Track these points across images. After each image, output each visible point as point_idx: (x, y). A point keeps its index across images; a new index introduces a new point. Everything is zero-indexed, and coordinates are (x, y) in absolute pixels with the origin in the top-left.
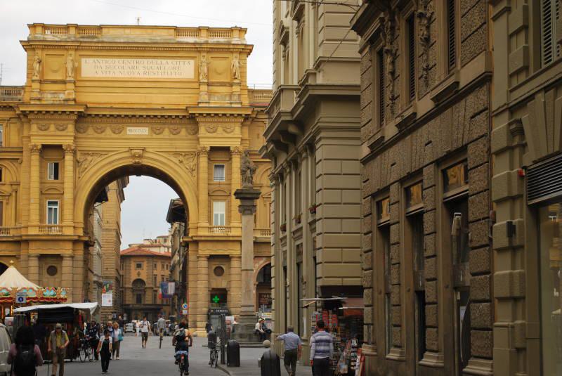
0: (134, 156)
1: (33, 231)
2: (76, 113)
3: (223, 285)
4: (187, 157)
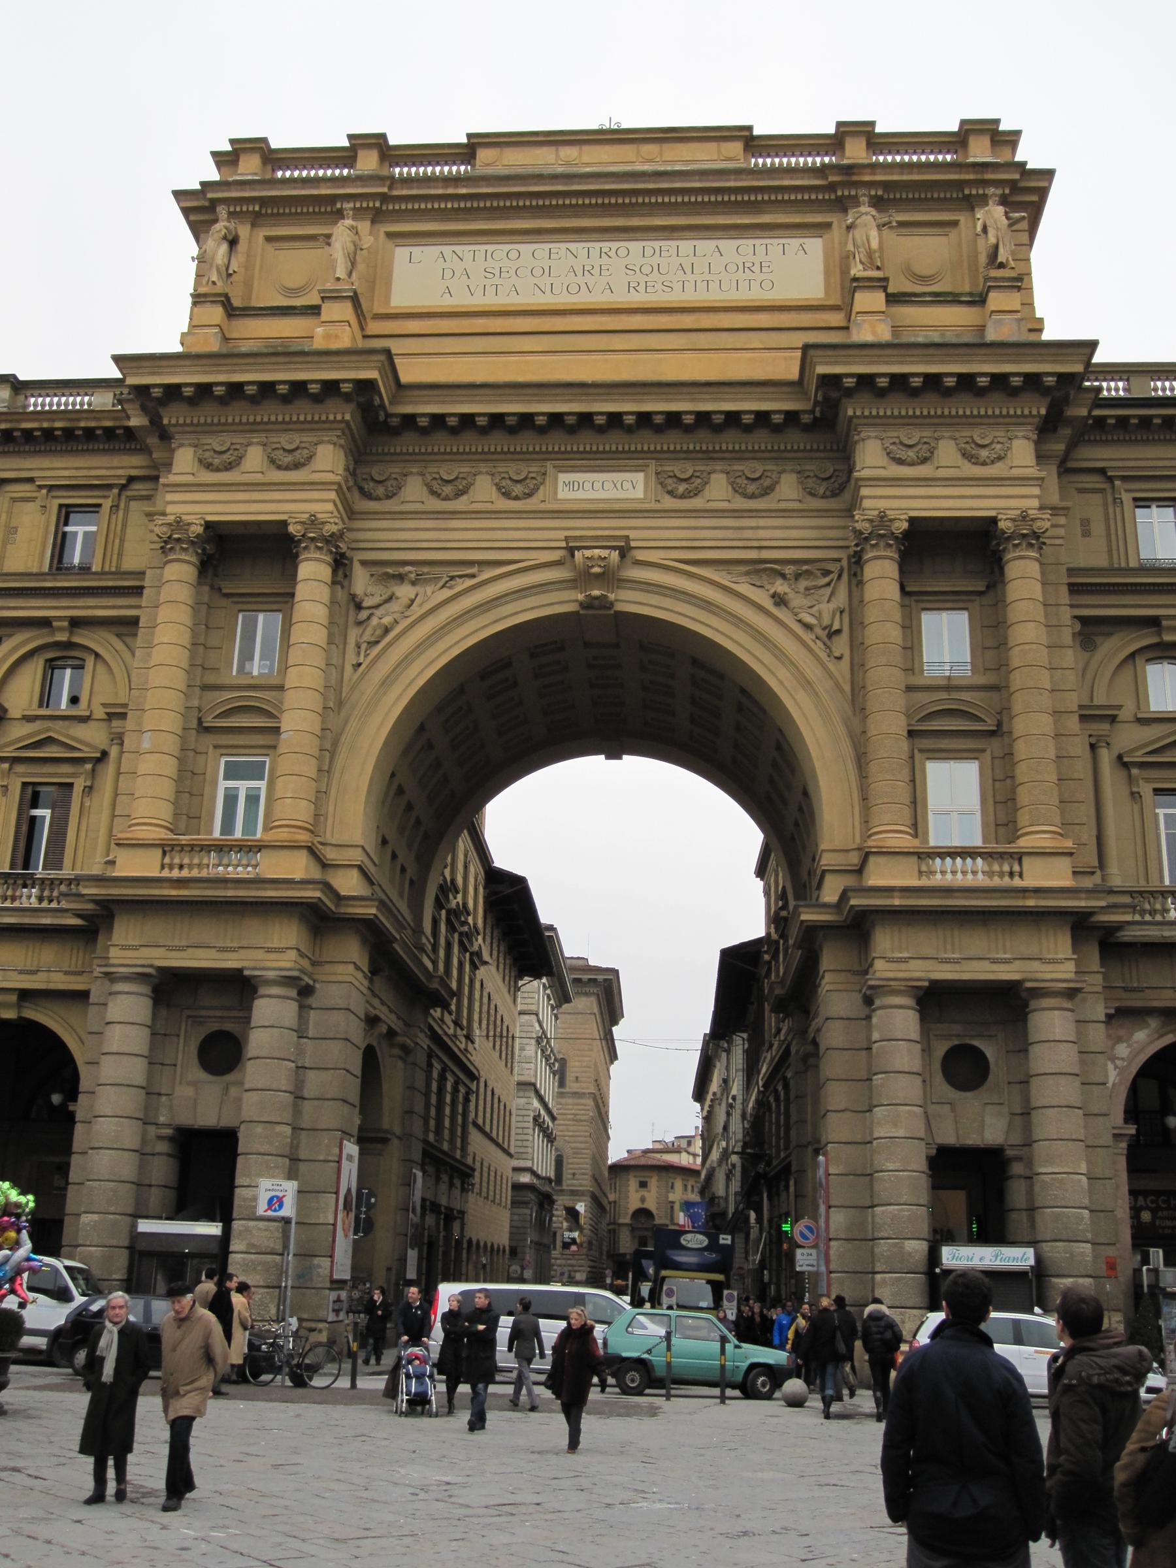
0: (584, 577)
2: (346, 388)
4: (803, 584)
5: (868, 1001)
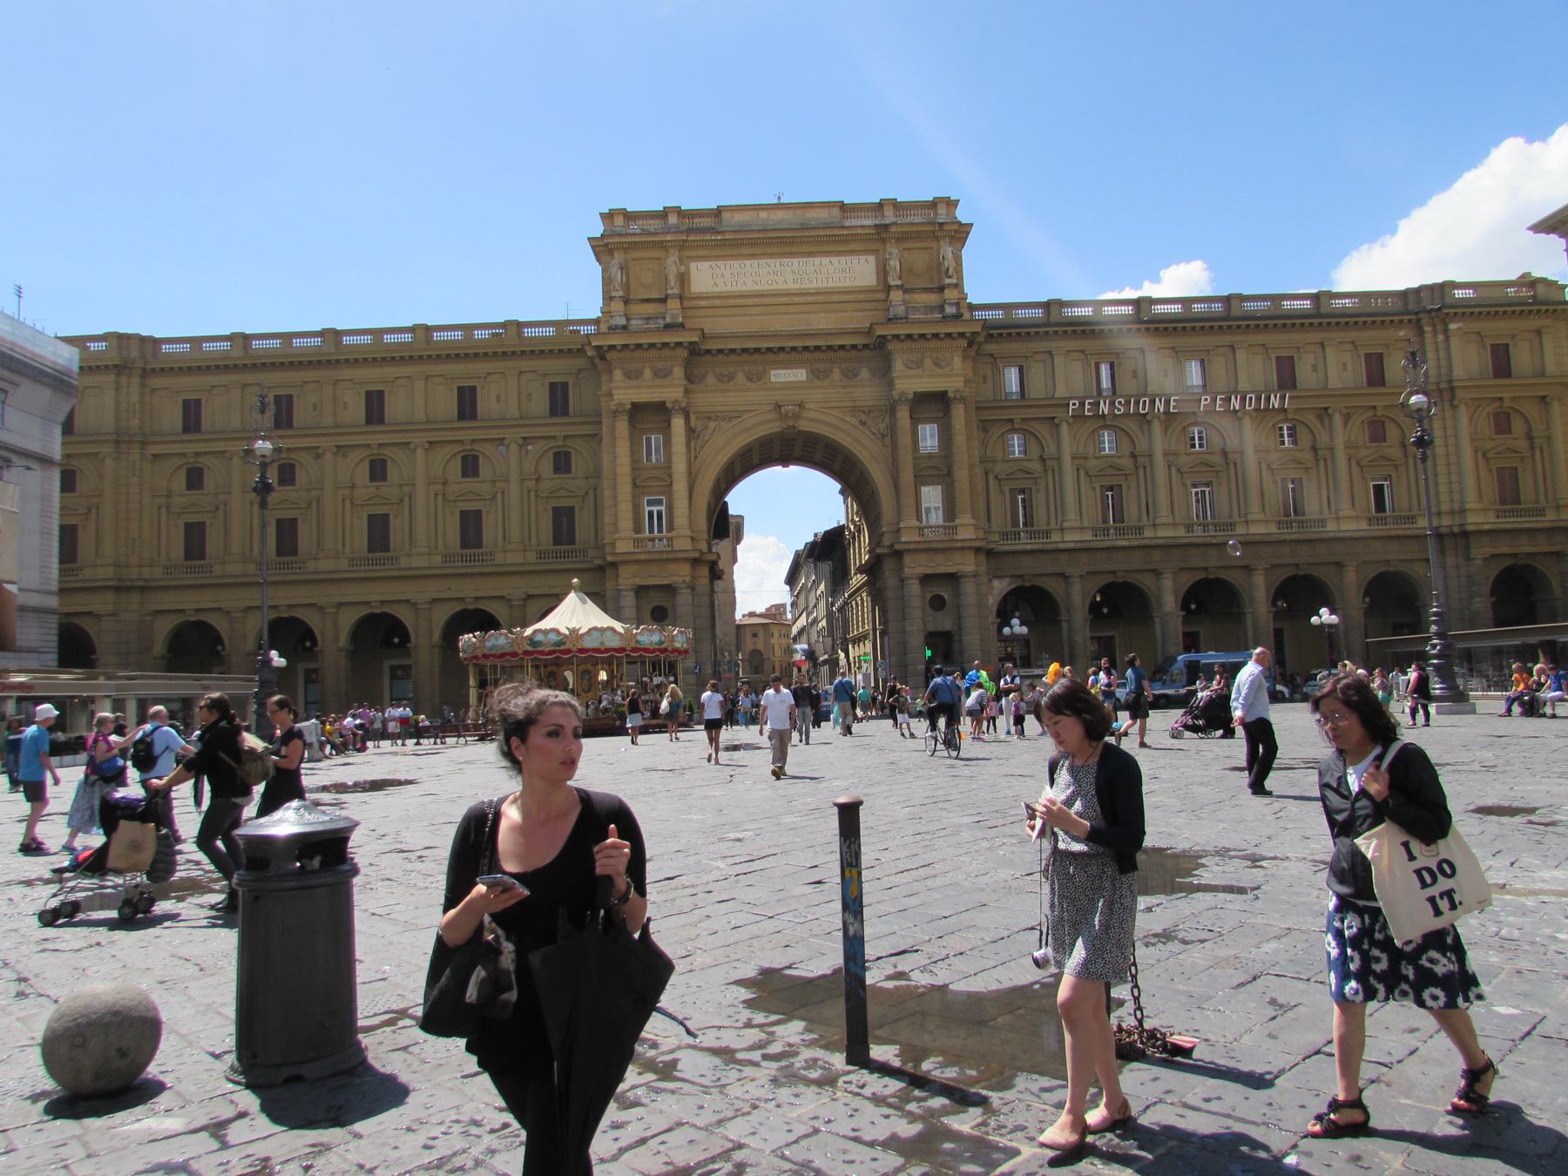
0: (783, 417)
1: (622, 547)
5: (902, 580)
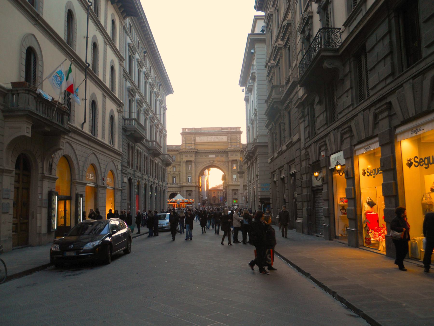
1: (184, 184)
3: (237, 198)
